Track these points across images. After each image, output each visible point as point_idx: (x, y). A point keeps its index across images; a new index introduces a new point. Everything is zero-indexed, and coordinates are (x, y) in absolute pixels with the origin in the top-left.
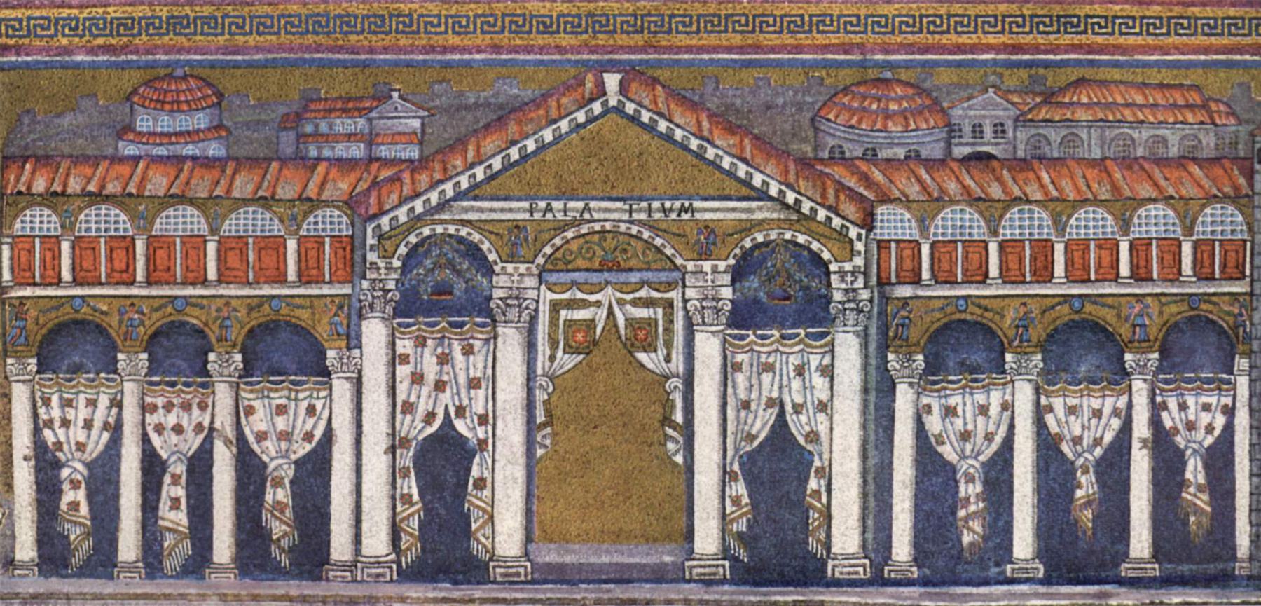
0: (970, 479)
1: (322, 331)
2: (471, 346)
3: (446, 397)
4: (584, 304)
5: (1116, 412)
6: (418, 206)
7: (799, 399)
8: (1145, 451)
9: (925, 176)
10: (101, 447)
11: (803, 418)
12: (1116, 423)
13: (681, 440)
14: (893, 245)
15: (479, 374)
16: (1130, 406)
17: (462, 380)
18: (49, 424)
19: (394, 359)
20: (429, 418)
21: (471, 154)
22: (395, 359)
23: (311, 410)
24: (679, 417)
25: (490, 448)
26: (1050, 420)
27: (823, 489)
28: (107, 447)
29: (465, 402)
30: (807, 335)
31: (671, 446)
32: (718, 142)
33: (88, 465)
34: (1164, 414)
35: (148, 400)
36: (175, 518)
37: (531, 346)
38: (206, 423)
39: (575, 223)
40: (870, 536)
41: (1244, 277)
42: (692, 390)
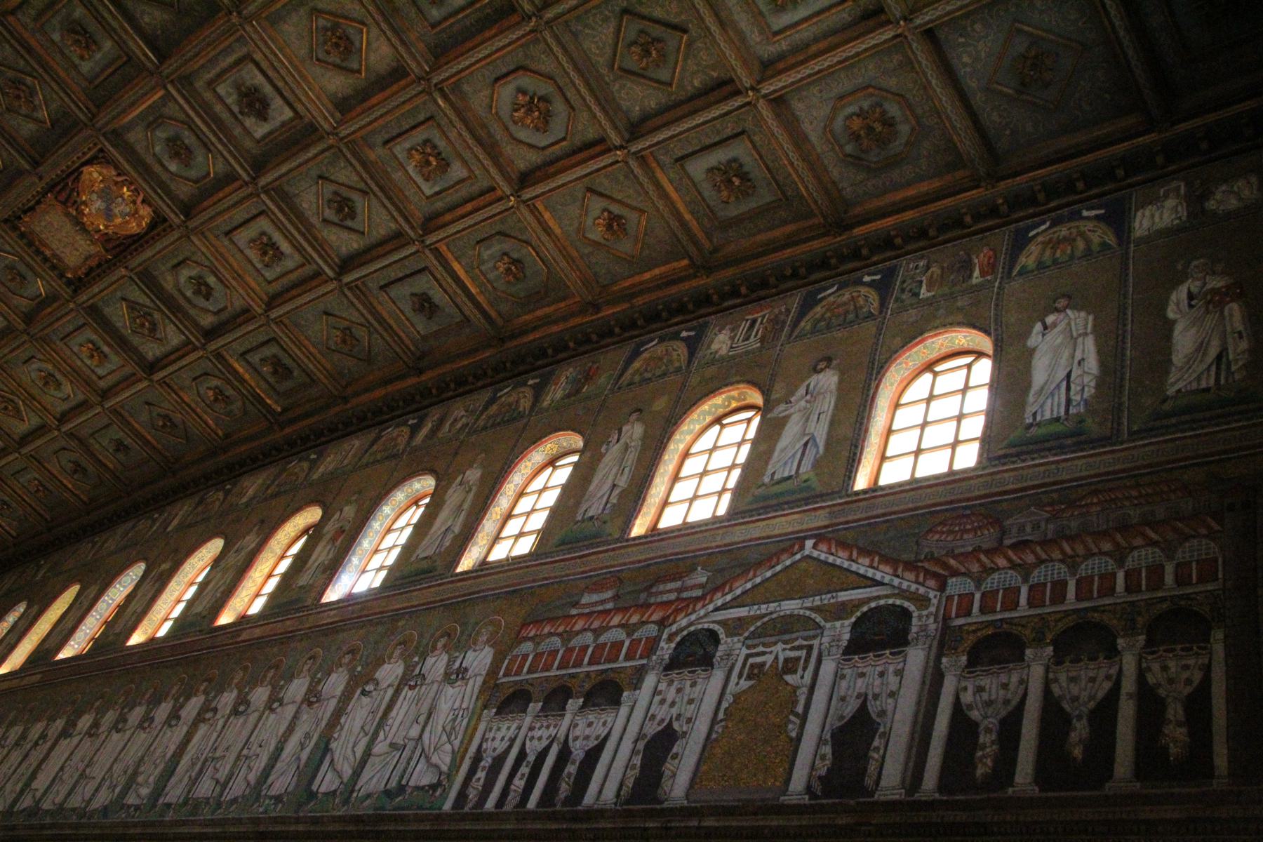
0: (988, 730)
4: (763, 653)
5: (1108, 677)
6: (693, 617)
7: (877, 690)
12: (1107, 685)
13: (798, 722)
17: (686, 699)
20: (663, 720)
22: (656, 692)
23: (604, 724)
24: (800, 709)
31: (790, 726)
36: (519, 783)
39: (771, 613)
41: (1217, 579)
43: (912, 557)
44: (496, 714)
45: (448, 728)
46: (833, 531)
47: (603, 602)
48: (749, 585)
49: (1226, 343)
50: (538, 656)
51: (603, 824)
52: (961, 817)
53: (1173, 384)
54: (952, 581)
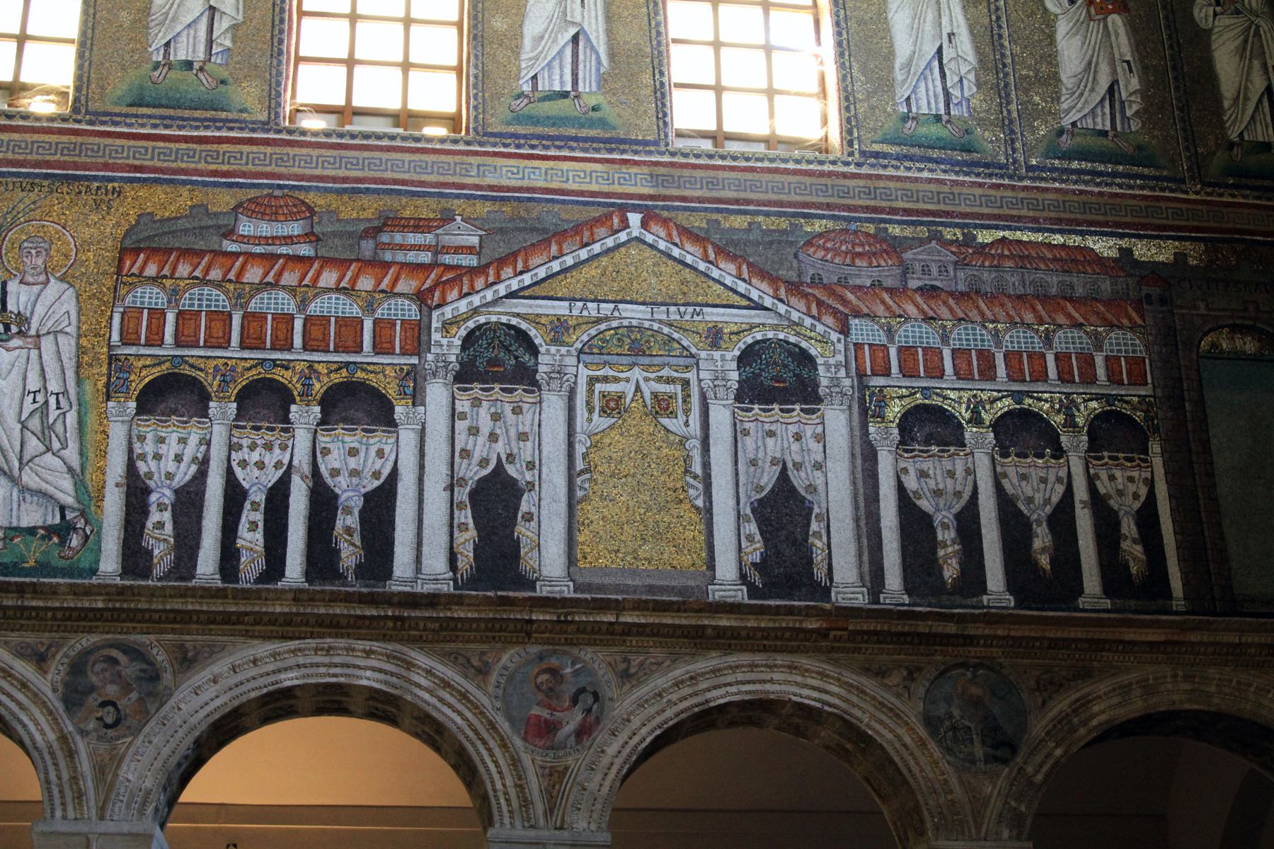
0: (945, 527)
1: (391, 391)
2: (521, 408)
3: (500, 447)
4: (617, 380)
5: (1059, 480)
6: (476, 300)
7: (798, 459)
8: (1086, 511)
9: (888, 300)
10: (188, 478)
11: (803, 474)
12: (1060, 489)
13: (700, 486)
14: (866, 347)
15: (527, 429)
16: (1069, 475)
18: (143, 457)
19: (453, 416)
20: (484, 462)
21: (520, 267)
22: (454, 415)
23: (380, 453)
24: (697, 468)
25: (537, 488)
26: (1006, 483)
27: (823, 532)
28: (194, 478)
29: (515, 451)
30: (802, 410)
31: (691, 492)
32: (721, 266)
33: (176, 492)
34: (1098, 483)
35: (235, 440)
36: (251, 538)
37: (571, 410)
38: (286, 461)
39: (607, 319)
40: (866, 568)
41: (1146, 384)
42: (708, 450)
43: (792, 275)
44: (141, 410)
45: (35, 423)
46: (663, 208)
47: (288, 240)
48: (556, 266)
49: (1114, 72)
50: (180, 315)
51: (460, 613)
52: (952, 628)
53: (1068, 111)
54: (854, 322)
